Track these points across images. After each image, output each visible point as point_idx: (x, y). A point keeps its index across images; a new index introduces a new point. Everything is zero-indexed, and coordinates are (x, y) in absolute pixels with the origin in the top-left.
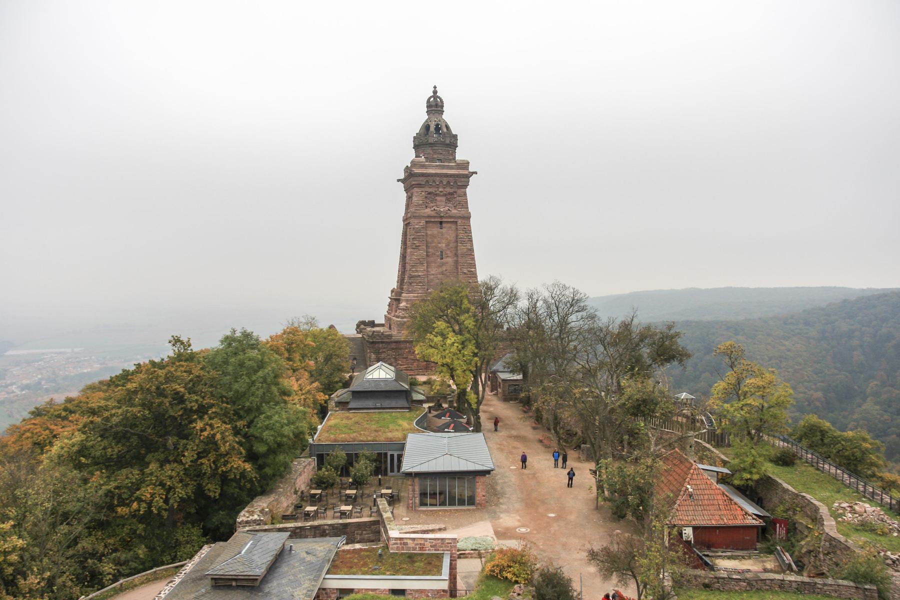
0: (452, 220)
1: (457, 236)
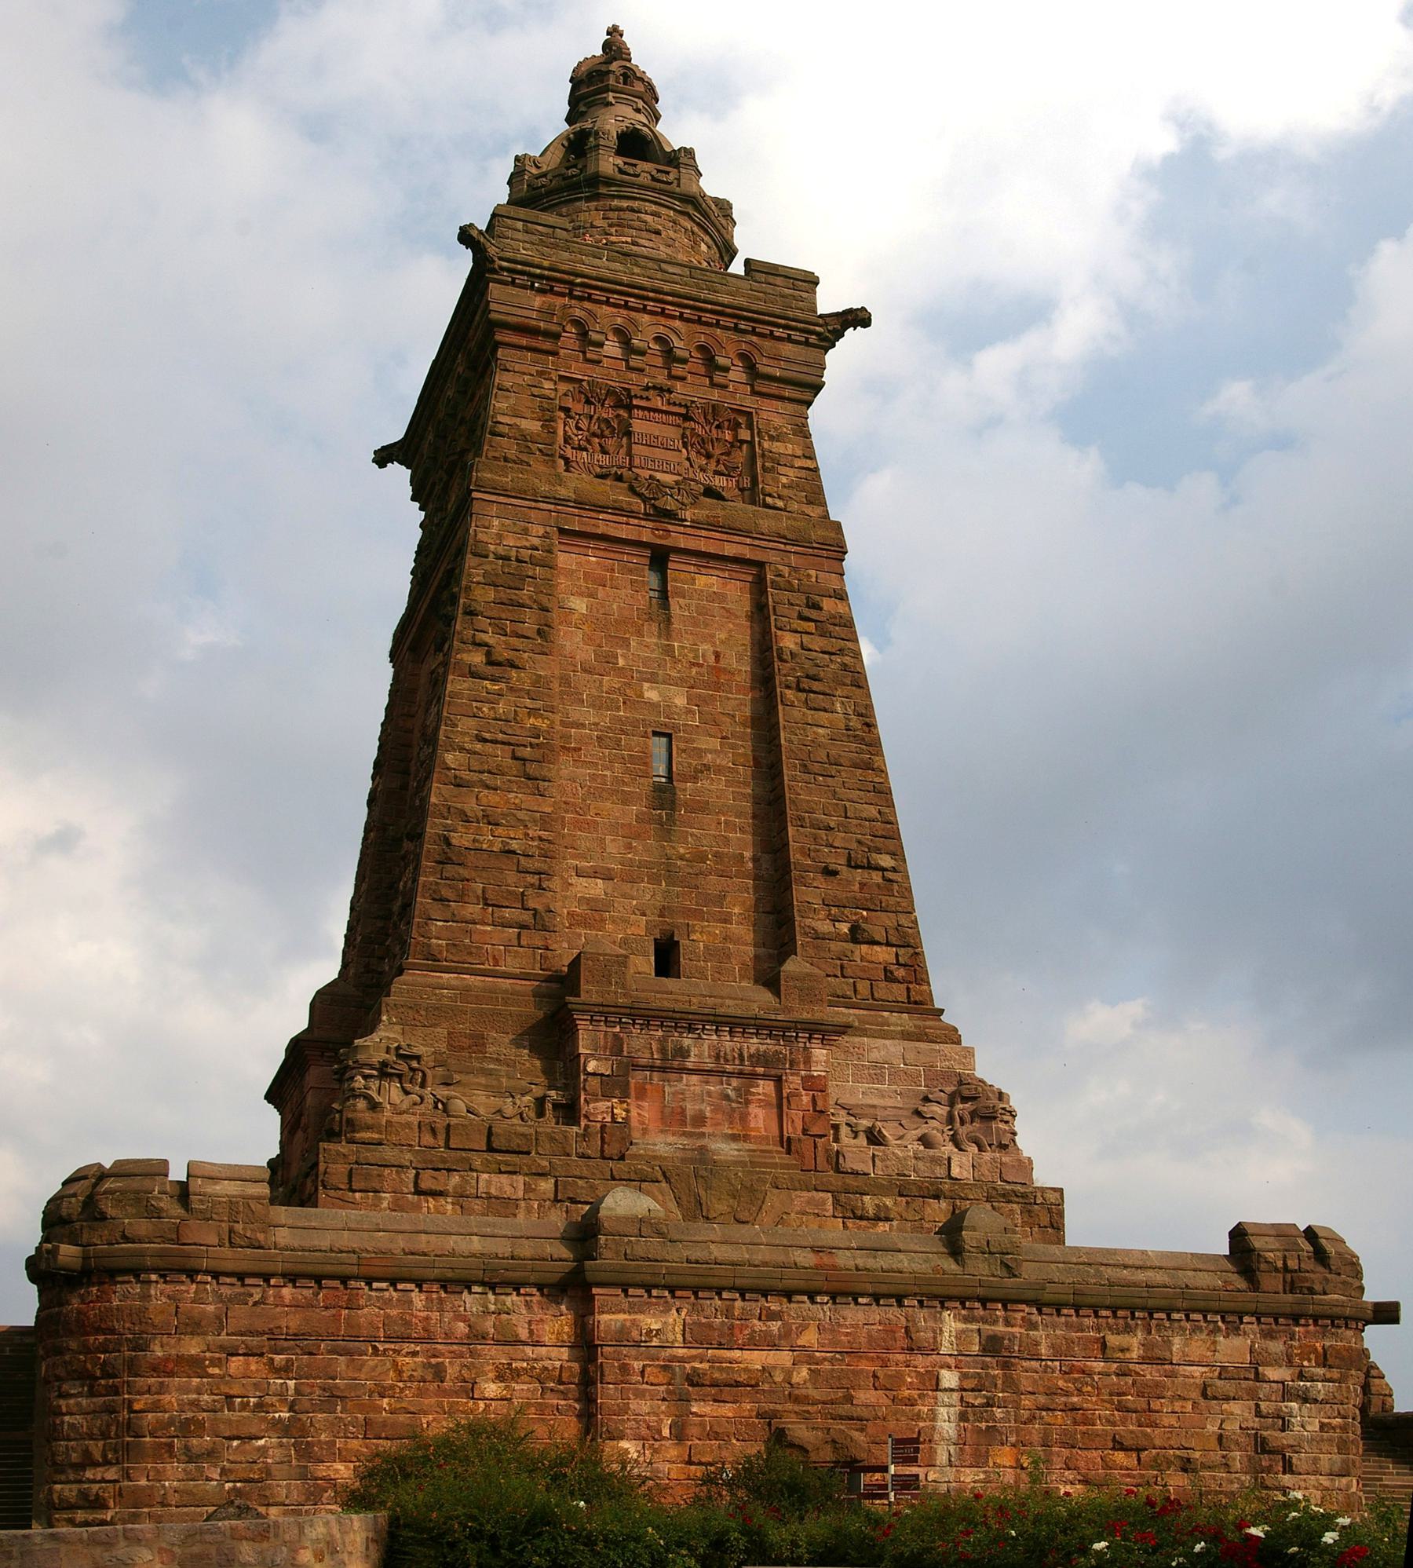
0: (730, 550)
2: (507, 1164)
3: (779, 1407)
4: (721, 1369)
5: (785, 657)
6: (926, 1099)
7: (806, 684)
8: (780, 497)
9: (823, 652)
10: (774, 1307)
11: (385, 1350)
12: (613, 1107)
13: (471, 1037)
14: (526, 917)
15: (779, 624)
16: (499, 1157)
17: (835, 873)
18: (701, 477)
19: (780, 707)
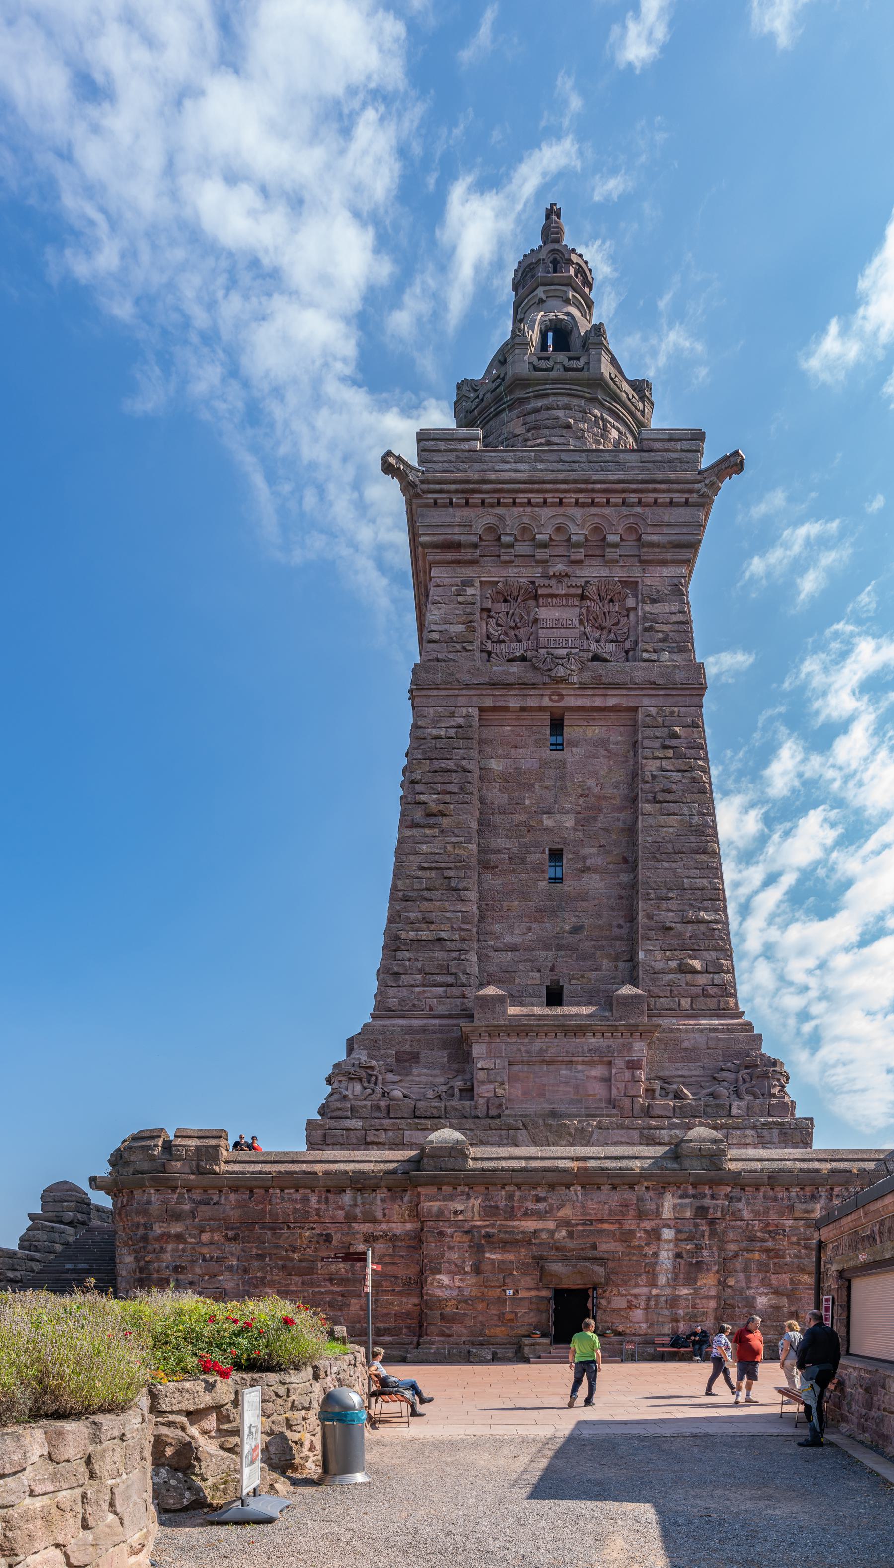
1: (635, 775)
3: (545, 1253)
4: (505, 1232)
5: (646, 778)
9: (679, 771)
10: (542, 1194)
11: (294, 1227)
15: (645, 754)
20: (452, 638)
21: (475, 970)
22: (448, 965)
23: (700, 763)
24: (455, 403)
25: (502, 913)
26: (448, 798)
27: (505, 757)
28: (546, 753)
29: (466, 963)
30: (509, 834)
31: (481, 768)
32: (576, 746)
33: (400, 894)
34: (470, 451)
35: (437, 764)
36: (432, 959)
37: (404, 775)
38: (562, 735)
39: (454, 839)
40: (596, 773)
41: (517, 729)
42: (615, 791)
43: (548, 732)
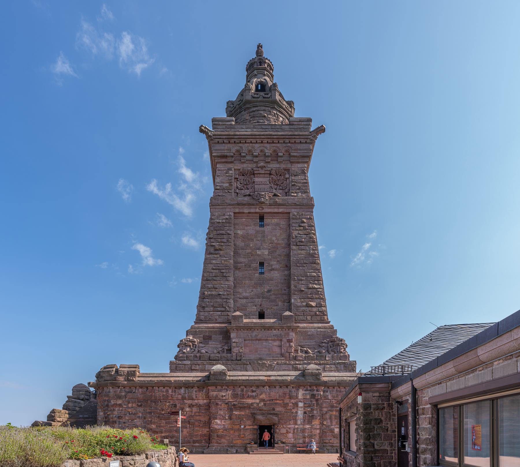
0: (281, 210)
1: (289, 236)
2: (212, 363)
5: (293, 237)
6: (323, 343)
7: (298, 244)
8: (296, 193)
9: (305, 235)
12: (239, 349)
13: (209, 336)
14: (223, 309)
16: (210, 361)
17: (303, 291)
18: (274, 191)
19: (291, 251)
20: (224, 188)
21: (232, 306)
22: (222, 304)
23: (313, 232)
24: (226, 109)
25: (242, 285)
26: (222, 244)
27: (243, 229)
28: (258, 228)
29: (229, 303)
30: (245, 257)
31: (234, 233)
32: (268, 226)
33: (205, 278)
34: (230, 125)
35: (219, 232)
36: (216, 302)
37: (207, 236)
38: (263, 222)
39: (225, 259)
40: (276, 235)
41: (247, 220)
42: (283, 242)
43: (259, 221)
